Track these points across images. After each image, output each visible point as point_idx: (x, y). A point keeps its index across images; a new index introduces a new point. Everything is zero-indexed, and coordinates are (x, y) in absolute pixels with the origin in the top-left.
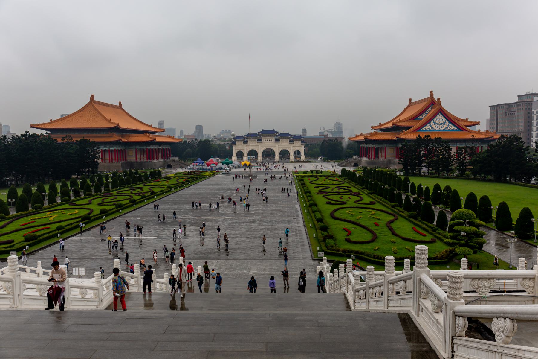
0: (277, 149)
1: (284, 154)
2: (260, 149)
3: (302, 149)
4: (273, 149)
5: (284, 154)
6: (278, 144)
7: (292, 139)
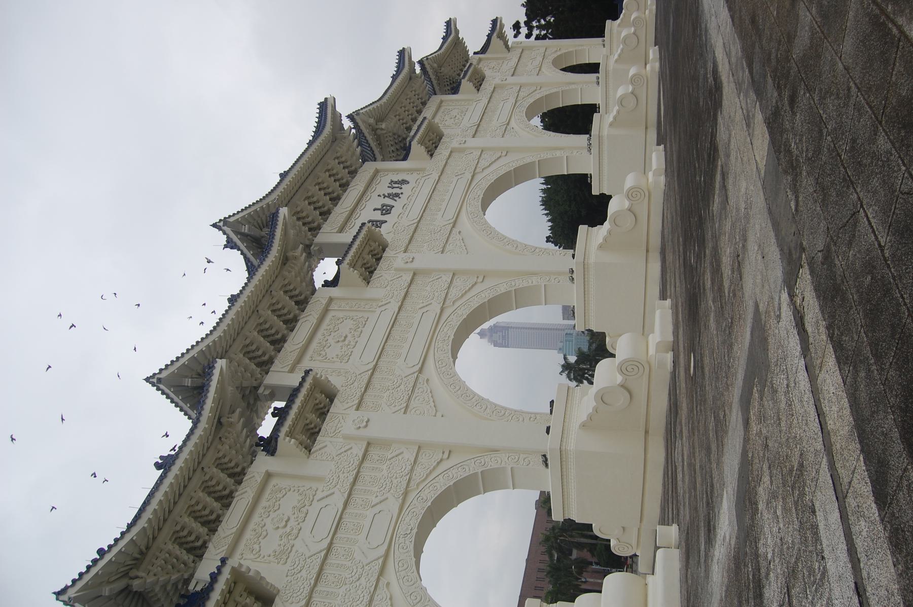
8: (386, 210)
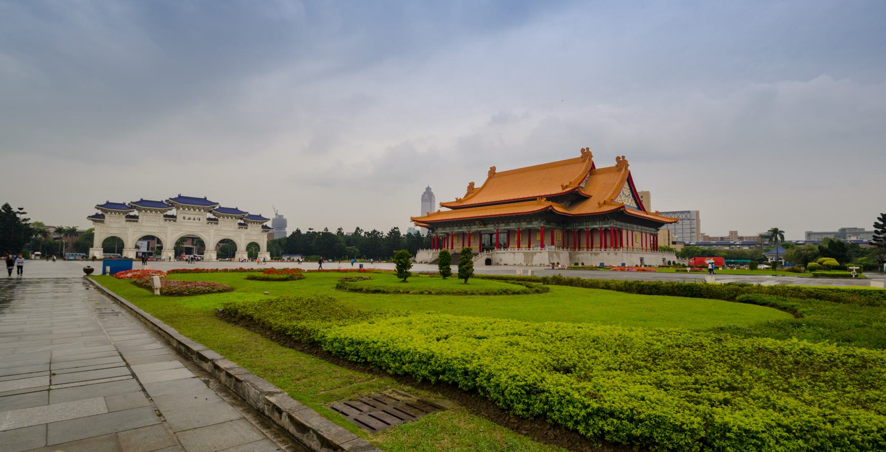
0: (211, 237)
2: (170, 235)
3: (263, 241)
6: (213, 228)
8: (189, 219)
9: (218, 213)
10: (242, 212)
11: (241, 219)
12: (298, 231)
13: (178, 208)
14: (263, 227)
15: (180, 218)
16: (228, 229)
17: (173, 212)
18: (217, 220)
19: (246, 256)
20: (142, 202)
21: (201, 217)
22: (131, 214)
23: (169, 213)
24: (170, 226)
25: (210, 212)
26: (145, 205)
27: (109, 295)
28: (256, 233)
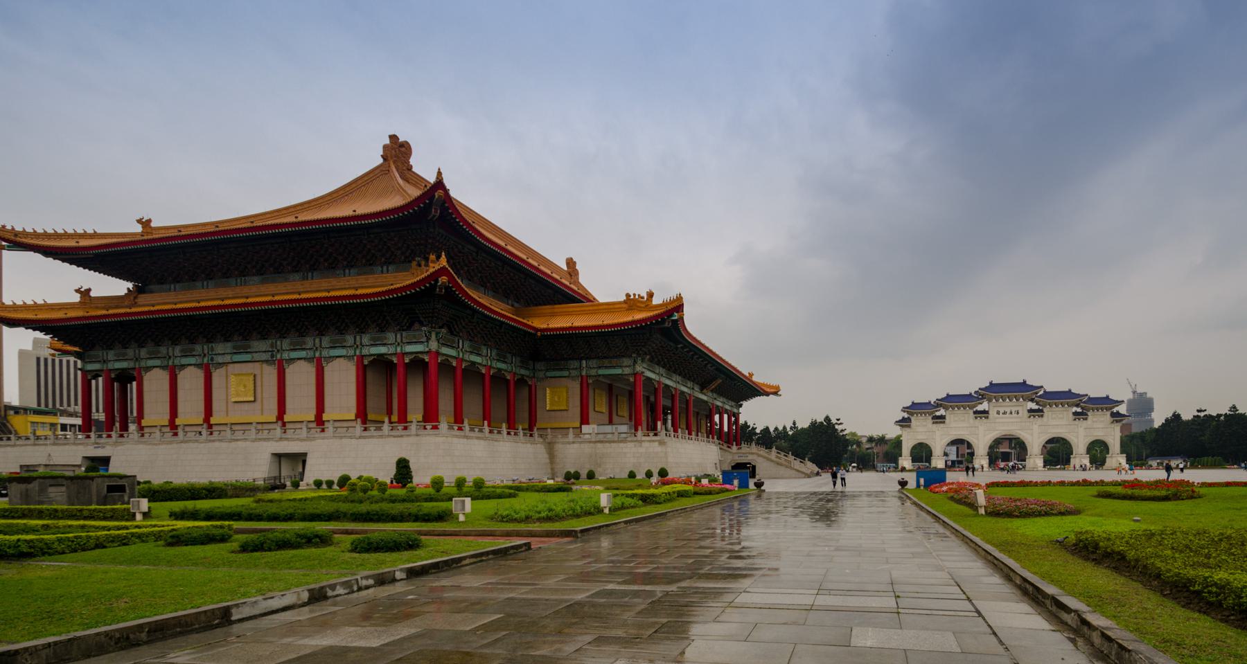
1: (1058, 453)
2: (982, 437)
3: (1113, 437)
4: (1024, 436)
5: (1058, 453)
7: (1083, 406)
8: (1005, 413)
9: (1041, 399)
10: (1078, 395)
11: (1077, 406)
12: (1176, 417)
13: (990, 401)
14: (1113, 415)
15: (993, 413)
16: (1058, 423)
17: (984, 406)
18: (1042, 411)
19: (1086, 462)
20: (949, 398)
21: (1020, 409)
22: (938, 414)
23: (980, 408)
24: (981, 424)
25: (1032, 400)
26: (953, 401)
27: (929, 512)
28: (1101, 425)
